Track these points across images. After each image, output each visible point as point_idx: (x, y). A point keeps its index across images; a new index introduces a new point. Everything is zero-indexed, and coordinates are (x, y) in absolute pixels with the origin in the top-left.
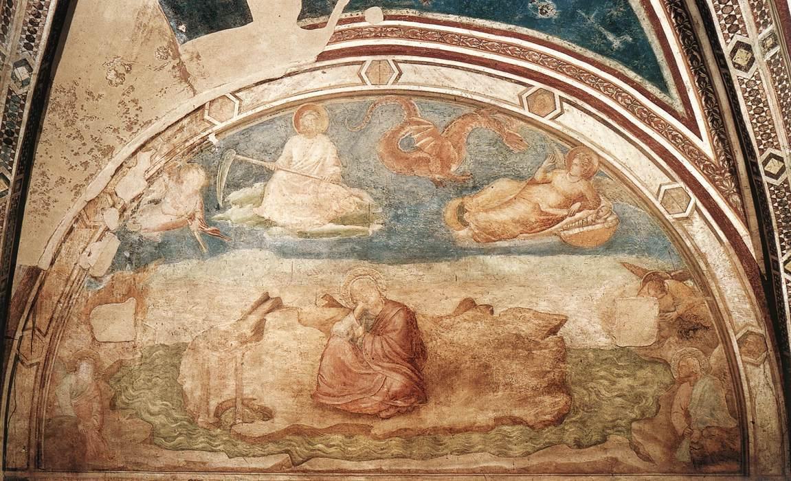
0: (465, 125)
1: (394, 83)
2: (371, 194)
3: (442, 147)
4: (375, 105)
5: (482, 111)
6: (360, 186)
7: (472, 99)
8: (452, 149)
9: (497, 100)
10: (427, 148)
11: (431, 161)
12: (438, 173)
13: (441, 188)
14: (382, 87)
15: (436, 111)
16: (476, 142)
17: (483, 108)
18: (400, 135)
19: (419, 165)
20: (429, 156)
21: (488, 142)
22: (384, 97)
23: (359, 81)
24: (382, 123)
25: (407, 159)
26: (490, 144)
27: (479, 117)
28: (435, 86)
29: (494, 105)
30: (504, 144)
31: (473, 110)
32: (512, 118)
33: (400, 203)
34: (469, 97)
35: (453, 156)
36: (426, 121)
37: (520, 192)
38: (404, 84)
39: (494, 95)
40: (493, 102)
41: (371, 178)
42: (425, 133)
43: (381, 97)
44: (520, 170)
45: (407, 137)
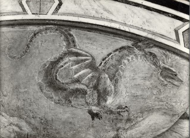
0: (122, 57)
1: (54, 13)
2: (29, 123)
3: (99, 79)
4: (35, 35)
5: (139, 44)
6: (20, 117)
7: (129, 33)
8: (108, 81)
9: (154, 34)
10: (85, 80)
11: (88, 93)
12: (95, 105)
13: (96, 120)
14: (42, 17)
15: (95, 43)
16: (132, 75)
17: (140, 41)
18: (59, 66)
19: (76, 97)
20: (86, 88)
21: (144, 76)
22: (44, 27)
23: (20, 9)
24: (41, 53)
25: (65, 90)
26: (145, 78)
27: (136, 51)
28: (94, 18)
29: (151, 39)
30: (159, 79)
31: (129, 43)
32: (168, 53)
33: (57, 133)
34: (127, 30)
35: (109, 89)
36: (84, 53)
37: (173, 126)
38: (64, 14)
39: (151, 29)
40: (150, 36)
41: (30, 108)
42: (83, 64)
43: (41, 27)
44: (174, 104)
45: (65, 68)
